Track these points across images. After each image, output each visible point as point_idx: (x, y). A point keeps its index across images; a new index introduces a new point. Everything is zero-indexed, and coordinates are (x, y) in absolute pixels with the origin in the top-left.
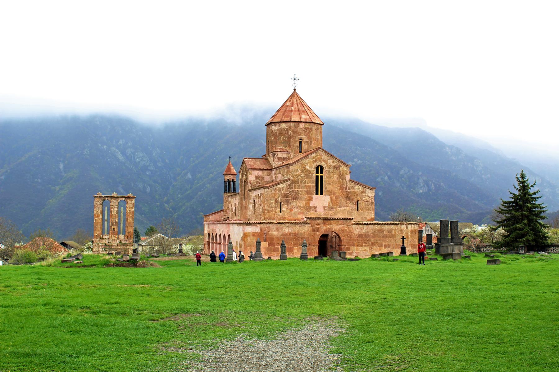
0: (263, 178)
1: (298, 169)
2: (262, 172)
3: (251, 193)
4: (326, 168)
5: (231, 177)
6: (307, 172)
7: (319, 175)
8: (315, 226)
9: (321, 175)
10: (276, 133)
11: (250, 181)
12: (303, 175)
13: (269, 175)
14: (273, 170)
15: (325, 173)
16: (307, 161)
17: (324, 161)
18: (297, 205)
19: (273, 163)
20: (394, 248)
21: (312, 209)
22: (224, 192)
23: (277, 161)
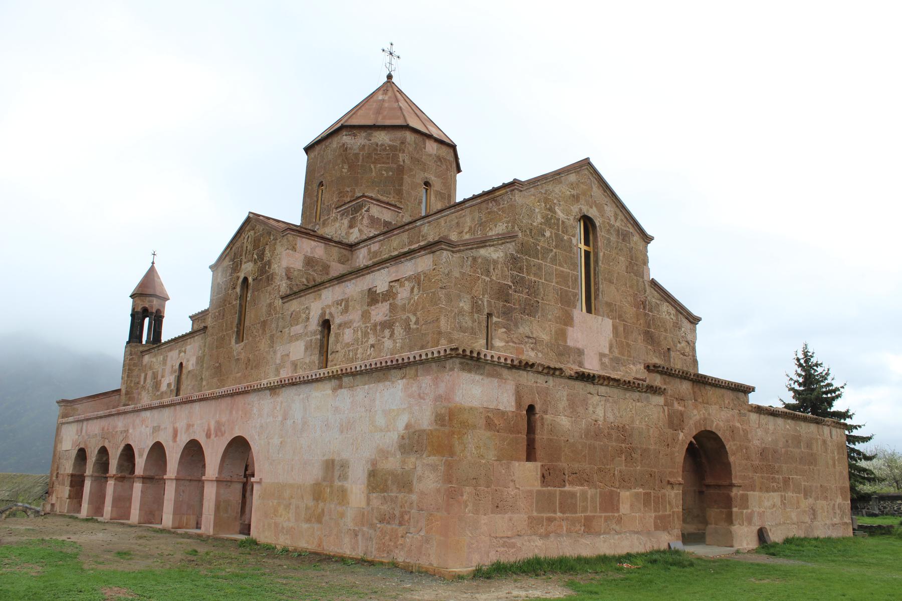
0: (326, 268)
1: (537, 210)
2: (325, 248)
3: (294, 305)
4: (601, 229)
5: (155, 302)
6: (558, 227)
7: (583, 246)
8: (672, 405)
9: (587, 248)
10: (356, 155)
11: (288, 270)
12: (548, 234)
13: (343, 263)
14: (362, 245)
15: (599, 244)
16: (557, 190)
17: (595, 206)
18: (534, 336)
19: (348, 234)
20: (817, 499)
21: (571, 357)
22: (128, 343)
23: (368, 226)
